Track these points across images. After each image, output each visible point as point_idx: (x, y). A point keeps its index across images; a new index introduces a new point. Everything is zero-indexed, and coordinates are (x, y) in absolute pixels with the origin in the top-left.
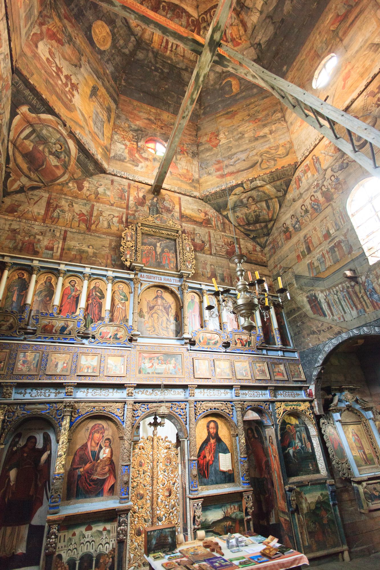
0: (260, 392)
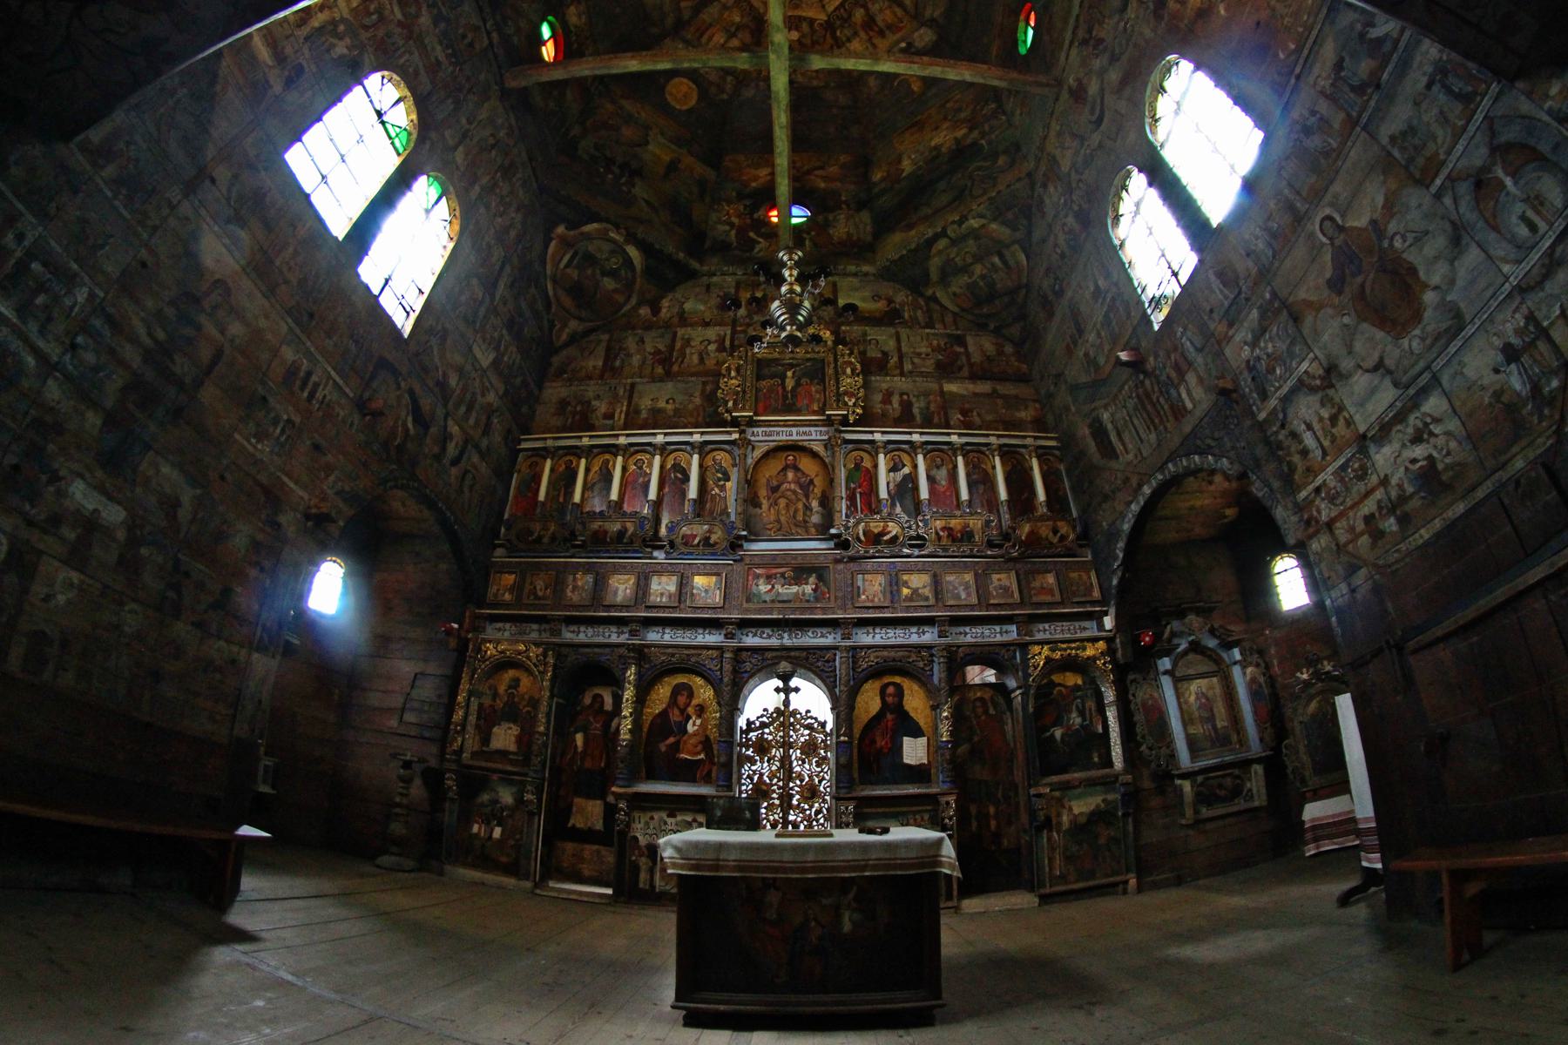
0: (998, 628)
